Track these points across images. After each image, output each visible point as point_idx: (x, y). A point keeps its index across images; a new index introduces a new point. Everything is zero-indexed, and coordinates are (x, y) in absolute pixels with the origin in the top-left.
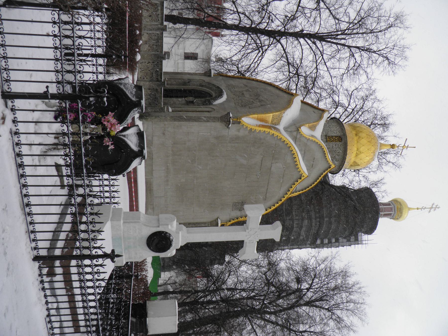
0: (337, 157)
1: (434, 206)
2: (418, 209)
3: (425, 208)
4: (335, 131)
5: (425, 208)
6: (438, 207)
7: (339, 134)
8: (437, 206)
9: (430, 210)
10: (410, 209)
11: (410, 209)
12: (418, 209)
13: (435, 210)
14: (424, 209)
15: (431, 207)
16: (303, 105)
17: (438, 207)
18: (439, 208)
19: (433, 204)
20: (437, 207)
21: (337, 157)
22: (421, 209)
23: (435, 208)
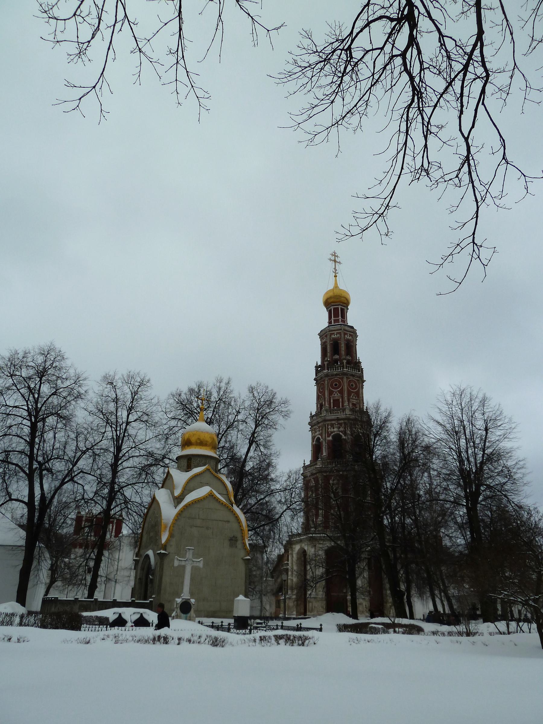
0: (203, 462)
1: (333, 258)
2: (336, 276)
3: (335, 269)
4: (184, 462)
5: (335, 269)
6: (333, 254)
7: (186, 461)
8: (332, 255)
9: (338, 262)
10: (336, 286)
11: (336, 286)
12: (336, 276)
13: (337, 256)
14: (336, 270)
15: (333, 262)
16: (164, 486)
17: (333, 254)
18: (335, 253)
19: (331, 260)
20: (334, 255)
21: (203, 462)
22: (335, 273)
23: (335, 256)
